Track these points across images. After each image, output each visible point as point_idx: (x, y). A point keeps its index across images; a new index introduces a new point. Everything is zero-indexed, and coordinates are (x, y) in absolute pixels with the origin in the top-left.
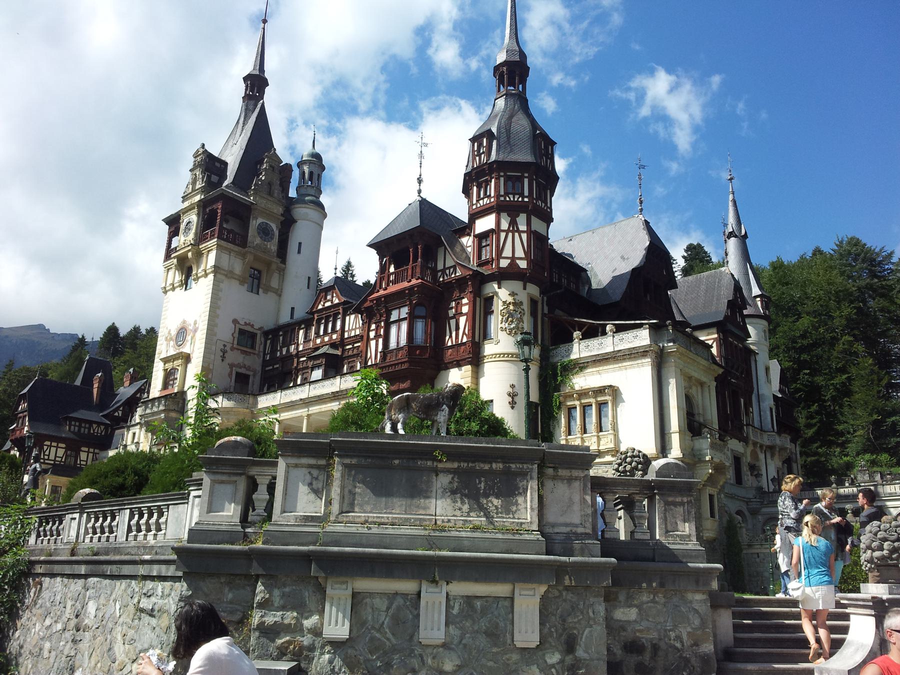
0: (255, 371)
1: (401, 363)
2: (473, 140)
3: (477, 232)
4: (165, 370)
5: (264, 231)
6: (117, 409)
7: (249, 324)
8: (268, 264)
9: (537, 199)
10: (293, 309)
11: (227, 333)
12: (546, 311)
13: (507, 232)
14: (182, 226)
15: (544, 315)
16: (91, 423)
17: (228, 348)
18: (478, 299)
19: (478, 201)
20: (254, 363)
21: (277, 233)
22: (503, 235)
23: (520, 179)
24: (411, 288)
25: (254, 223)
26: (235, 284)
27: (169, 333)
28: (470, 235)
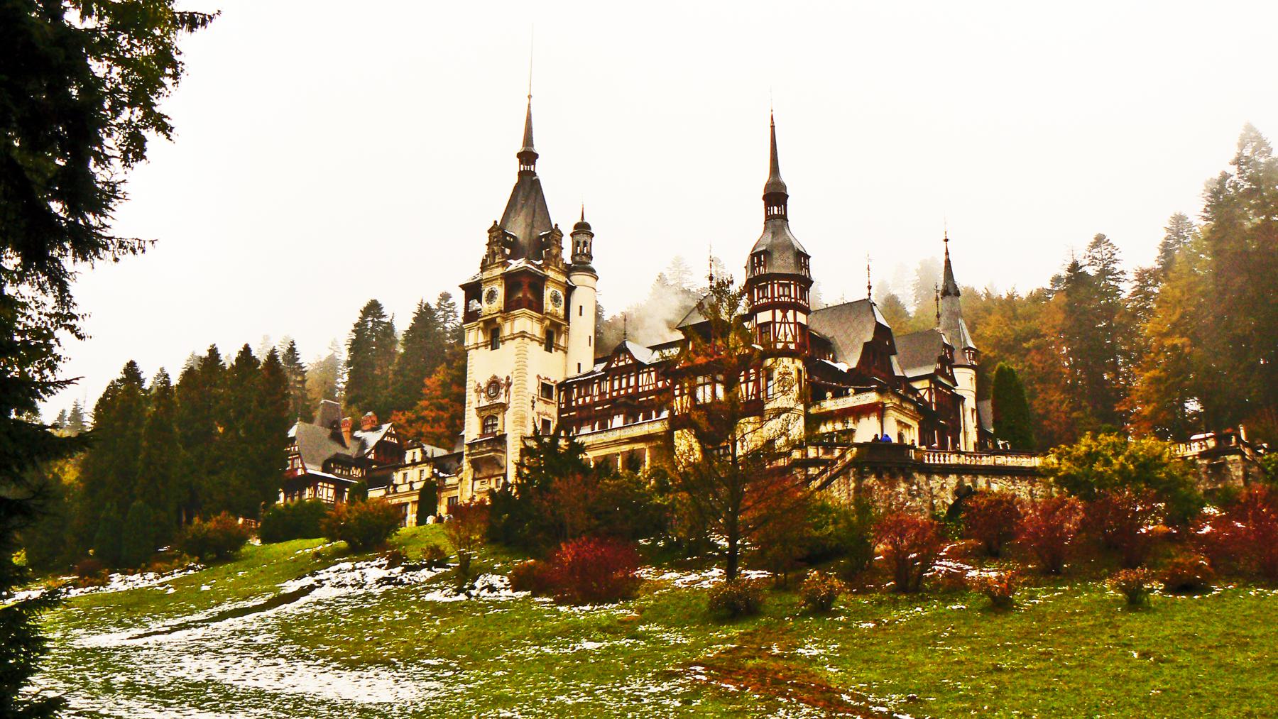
2: (753, 255)
5: (555, 299)
6: (369, 453)
8: (558, 326)
11: (533, 388)
14: (484, 294)
20: (552, 411)
21: (563, 299)
23: (788, 286)
25: (547, 294)
27: (479, 385)
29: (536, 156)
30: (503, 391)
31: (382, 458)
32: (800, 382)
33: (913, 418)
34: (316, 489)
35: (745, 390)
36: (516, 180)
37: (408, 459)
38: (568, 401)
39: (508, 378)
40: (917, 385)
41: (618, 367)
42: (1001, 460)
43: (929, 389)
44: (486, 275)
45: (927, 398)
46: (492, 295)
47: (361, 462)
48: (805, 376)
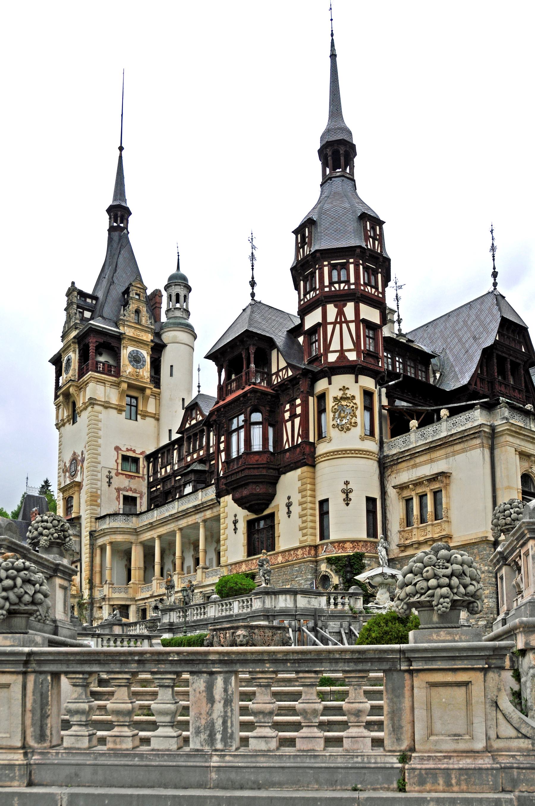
1: (242, 471)
4: (64, 499)
7: (131, 450)
11: (110, 460)
12: (385, 402)
15: (382, 407)
17: (113, 474)
18: (311, 399)
20: (140, 487)
24: (245, 395)
26: (115, 412)
30: (79, 468)
32: (369, 408)
35: (291, 432)
38: (155, 472)
41: (192, 427)
48: (381, 399)
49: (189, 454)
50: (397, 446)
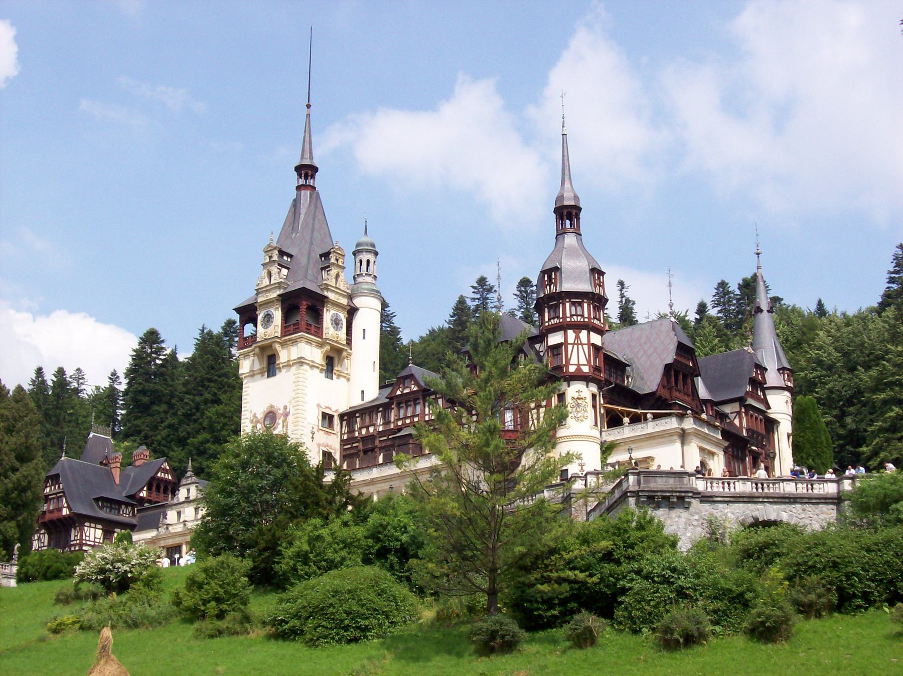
0: (335, 450)
2: (543, 272)
3: (550, 344)
5: (336, 322)
6: (142, 490)
8: (339, 351)
9: (594, 318)
10: (363, 392)
12: (602, 402)
13: (574, 344)
15: (600, 404)
16: (119, 503)
17: (315, 430)
19: (549, 320)
22: (570, 347)
23: (581, 304)
25: (328, 315)
27: (255, 416)
28: (541, 342)
29: (315, 169)
31: (154, 494)
32: (594, 407)
33: (717, 444)
34: (82, 530)
35: (537, 419)
36: (293, 194)
37: (182, 494)
38: (351, 431)
39: (285, 408)
40: (727, 409)
41: (403, 395)
42: (789, 488)
43: (739, 413)
44: (261, 299)
45: (737, 422)
46: (268, 318)
47: (134, 501)
48: (600, 400)
49: (399, 419)
50: (613, 435)
